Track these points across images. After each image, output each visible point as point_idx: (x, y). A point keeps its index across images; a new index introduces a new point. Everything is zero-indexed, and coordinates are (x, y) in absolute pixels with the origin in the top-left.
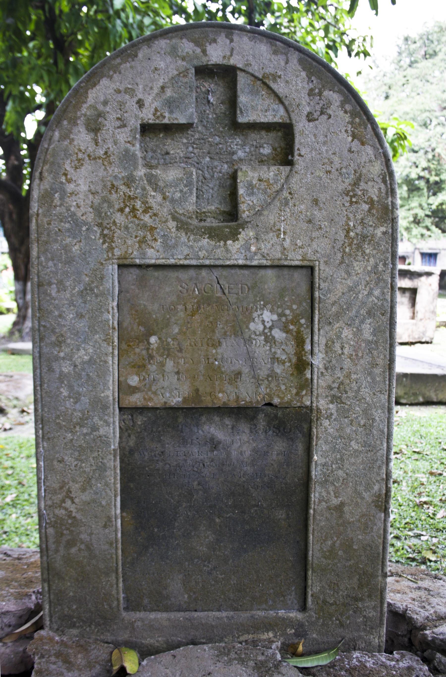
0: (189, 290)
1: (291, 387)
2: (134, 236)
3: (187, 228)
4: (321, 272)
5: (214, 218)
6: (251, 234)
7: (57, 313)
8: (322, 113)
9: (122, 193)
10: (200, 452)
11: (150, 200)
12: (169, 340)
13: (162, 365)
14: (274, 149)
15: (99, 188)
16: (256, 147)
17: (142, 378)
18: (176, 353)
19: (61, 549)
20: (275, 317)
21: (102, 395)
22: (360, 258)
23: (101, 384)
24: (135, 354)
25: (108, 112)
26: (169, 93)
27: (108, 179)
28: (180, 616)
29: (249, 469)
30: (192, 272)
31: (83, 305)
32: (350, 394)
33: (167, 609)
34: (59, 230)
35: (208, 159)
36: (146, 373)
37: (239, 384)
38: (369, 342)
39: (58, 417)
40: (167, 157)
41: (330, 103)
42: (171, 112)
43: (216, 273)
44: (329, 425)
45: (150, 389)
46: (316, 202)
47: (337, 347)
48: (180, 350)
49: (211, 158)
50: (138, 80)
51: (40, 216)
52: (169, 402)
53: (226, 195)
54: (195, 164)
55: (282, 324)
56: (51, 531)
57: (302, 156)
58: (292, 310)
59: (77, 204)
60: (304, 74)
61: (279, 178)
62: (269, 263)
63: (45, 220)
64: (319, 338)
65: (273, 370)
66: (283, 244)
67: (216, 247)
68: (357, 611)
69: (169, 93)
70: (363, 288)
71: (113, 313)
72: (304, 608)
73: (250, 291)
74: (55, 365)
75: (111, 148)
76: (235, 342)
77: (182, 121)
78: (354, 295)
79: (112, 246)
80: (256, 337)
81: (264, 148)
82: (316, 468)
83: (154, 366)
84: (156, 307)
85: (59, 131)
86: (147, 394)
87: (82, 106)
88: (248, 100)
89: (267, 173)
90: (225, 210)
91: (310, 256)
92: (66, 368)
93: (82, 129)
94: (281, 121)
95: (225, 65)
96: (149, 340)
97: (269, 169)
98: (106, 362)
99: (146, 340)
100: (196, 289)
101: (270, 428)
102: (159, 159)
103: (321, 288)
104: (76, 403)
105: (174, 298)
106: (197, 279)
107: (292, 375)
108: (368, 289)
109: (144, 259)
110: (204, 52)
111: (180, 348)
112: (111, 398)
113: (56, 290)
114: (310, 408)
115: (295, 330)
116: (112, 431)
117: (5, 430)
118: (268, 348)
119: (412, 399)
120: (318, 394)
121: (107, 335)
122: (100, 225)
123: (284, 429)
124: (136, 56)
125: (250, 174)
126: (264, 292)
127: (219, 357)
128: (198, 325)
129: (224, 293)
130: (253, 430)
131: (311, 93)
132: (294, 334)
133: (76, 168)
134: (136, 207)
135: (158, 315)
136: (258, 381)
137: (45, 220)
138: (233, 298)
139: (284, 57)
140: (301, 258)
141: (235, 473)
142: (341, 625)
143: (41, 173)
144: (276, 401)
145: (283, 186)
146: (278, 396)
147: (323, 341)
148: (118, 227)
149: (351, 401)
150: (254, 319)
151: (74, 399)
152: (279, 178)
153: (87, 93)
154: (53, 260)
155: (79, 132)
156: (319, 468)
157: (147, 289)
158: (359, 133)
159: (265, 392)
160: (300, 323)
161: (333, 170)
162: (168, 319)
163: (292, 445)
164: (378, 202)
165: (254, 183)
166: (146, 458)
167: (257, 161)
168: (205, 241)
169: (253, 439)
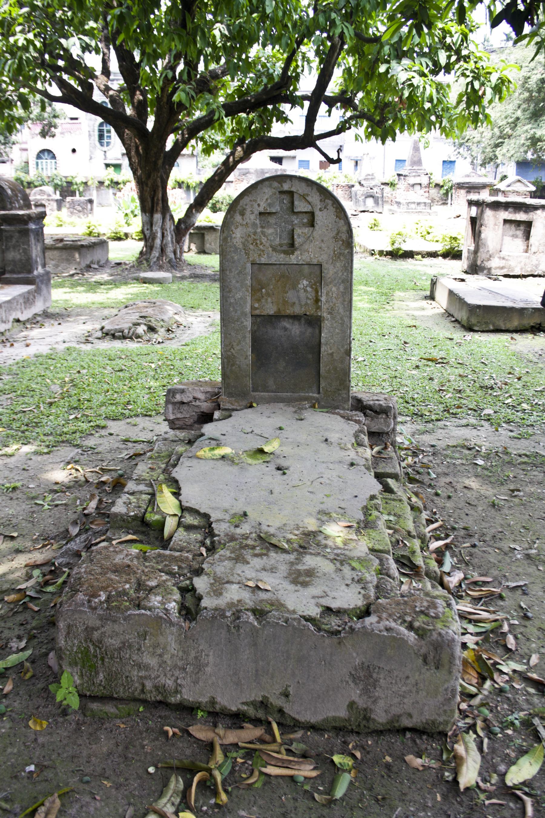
13: (267, 300)
19: (230, 368)
26: (269, 201)
28: (273, 394)
29: (298, 339)
30: (278, 266)
33: (268, 392)
38: (342, 292)
41: (328, 204)
43: (287, 266)
46: (322, 241)
47: (330, 294)
56: (225, 360)
68: (339, 394)
69: (269, 201)
72: (319, 393)
74: (228, 300)
77: (274, 211)
92: (232, 301)
93: (238, 214)
105: (271, 275)
110: (282, 186)
114: (321, 316)
117: (159, 343)
119: (484, 327)
122: (244, 249)
130: (300, 324)
131: (321, 201)
136: (301, 306)
138: (292, 276)
142: (333, 400)
144: (308, 313)
168: (282, 255)
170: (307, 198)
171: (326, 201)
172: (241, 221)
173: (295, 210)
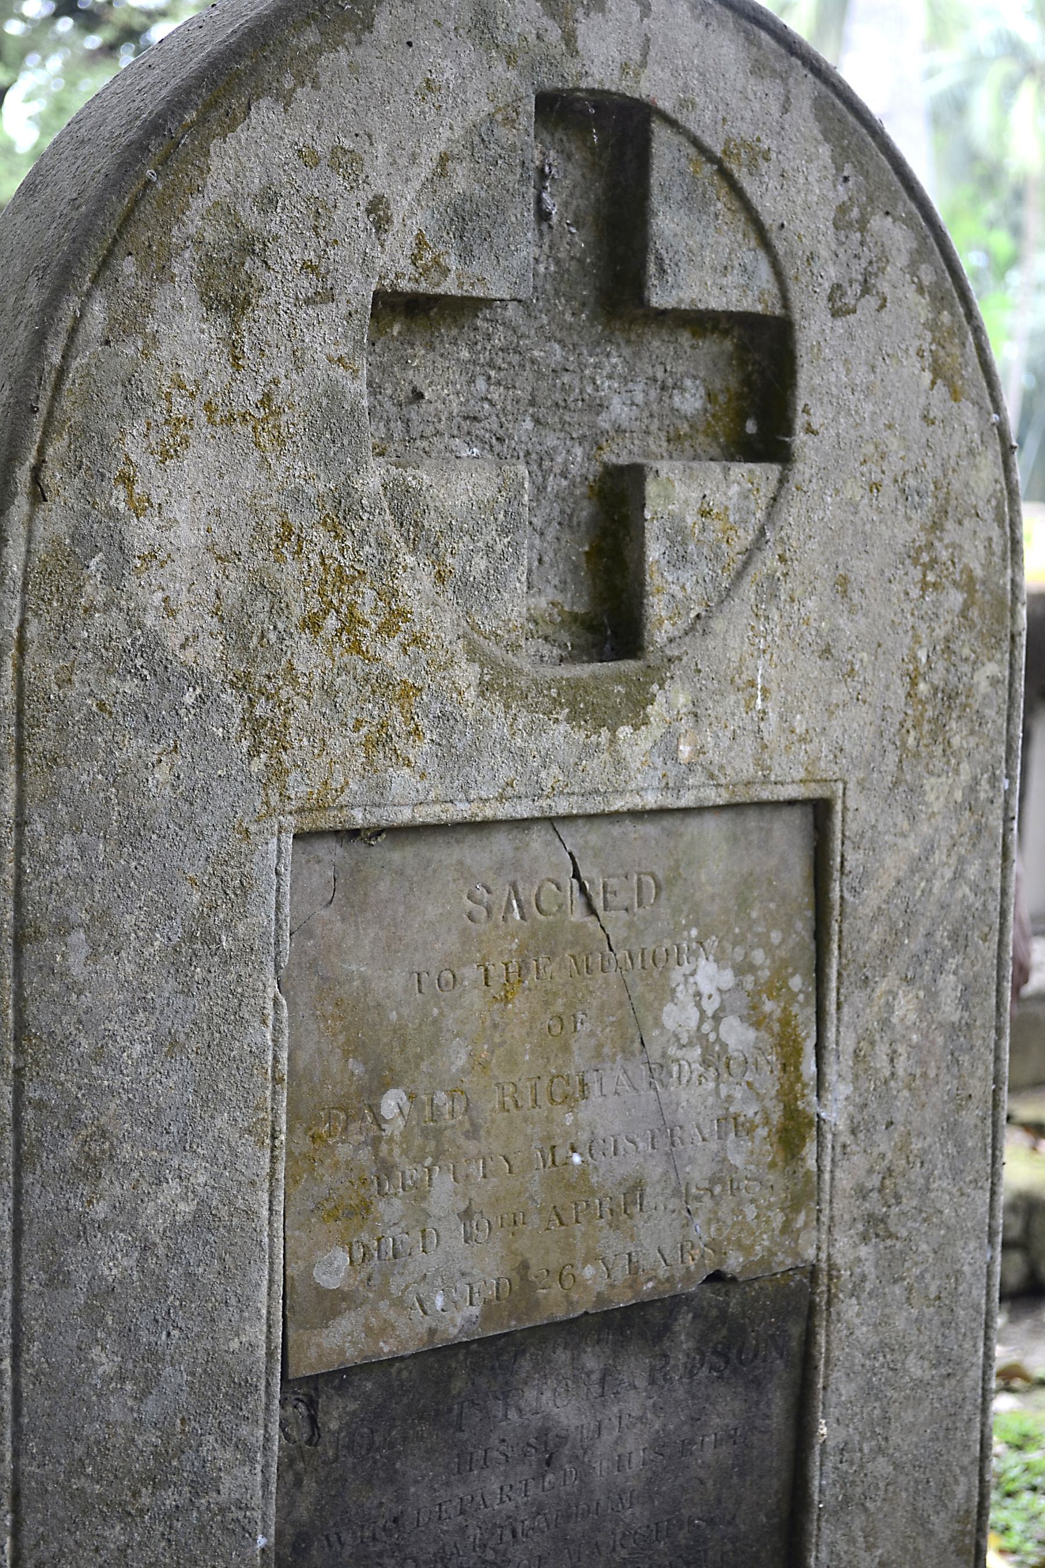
0: (495, 910)
1: (770, 1207)
2: (351, 723)
3: (510, 686)
4: (850, 815)
5: (546, 639)
6: (682, 700)
7: (86, 1045)
8: (866, 290)
9: (315, 559)
10: (507, 1489)
11: (405, 585)
12: (441, 1097)
13: (420, 1193)
14: (710, 396)
15: (241, 538)
16: (663, 388)
17: (359, 1254)
18: (462, 1141)
20: (727, 978)
21: (235, 1345)
22: (939, 764)
23: (233, 1301)
24: (336, 1165)
25: (276, 238)
27: (272, 501)
30: (502, 843)
31: (179, 1002)
32: (909, 1203)
34: (101, 706)
35: (528, 425)
36: (372, 1231)
37: (639, 1220)
39: (77, 1468)
40: (413, 413)
41: (884, 258)
42: (466, 255)
43: (573, 837)
44: (858, 1315)
45: (384, 1293)
48: (473, 1133)
49: (537, 421)
50: (374, 122)
51: (32, 649)
52: (442, 1327)
53: (578, 554)
54: (494, 441)
55: (746, 1000)
57: (815, 433)
58: (770, 949)
59: (166, 600)
60: (825, 151)
61: (752, 506)
62: (722, 797)
63: (52, 666)
64: (838, 1031)
65: (725, 1159)
66: (759, 730)
67: (589, 751)
69: (461, 179)
70: (944, 857)
71: (277, 1020)
73: (664, 895)
74: (74, 1258)
75: (283, 381)
76: (623, 1078)
78: (923, 884)
79: (280, 762)
80: (680, 1054)
81: (683, 390)
82: (822, 1465)
83: (396, 1202)
84: (398, 979)
85: (108, 297)
86: (375, 1310)
87: (188, 206)
88: (678, 230)
89: (723, 487)
90: (576, 609)
91: (826, 768)
93: (188, 298)
94: (759, 308)
95: (624, 96)
96: (379, 1106)
97: (726, 471)
98: (250, 1213)
99: (370, 1107)
100: (514, 902)
101: (703, 1355)
102: (389, 421)
103: (847, 868)
104: (141, 1397)
106: (517, 865)
107: (772, 1165)
108: (953, 861)
109: (379, 806)
110: (569, 38)
111: (472, 1124)
112: (262, 1352)
113: (86, 950)
115: (778, 1013)
116: (259, 1478)
118: (711, 1085)
120: (832, 1218)
121: (257, 1108)
122: (241, 683)
123: (740, 1352)
124: (369, 27)
125: (680, 490)
126: (698, 896)
127: (584, 1137)
128: (524, 1031)
129: (592, 910)
131: (841, 222)
132: (776, 1027)
133: (166, 455)
134: (357, 612)
135: (405, 1011)
137: (52, 666)
139: (778, 88)
140: (802, 774)
141: (600, 1538)
143: (36, 472)
144: (734, 1263)
145: (762, 532)
146: (740, 1246)
147: (849, 1043)
148: (302, 690)
149: (910, 1224)
150: (673, 991)
151: (136, 1383)
152: (752, 506)
153: (207, 154)
154: (76, 830)
155: (177, 307)
156: (831, 1461)
157: (369, 915)
158: (949, 360)
159: (706, 1239)
160: (789, 989)
161: (887, 481)
162: (435, 1022)
163: (757, 1403)
164: (984, 583)
165: (689, 521)
166: (348, 1550)
167: (663, 435)
169: (654, 1405)
170: (749, 186)
171: (878, 223)
172: (218, 377)
173: (659, 298)
